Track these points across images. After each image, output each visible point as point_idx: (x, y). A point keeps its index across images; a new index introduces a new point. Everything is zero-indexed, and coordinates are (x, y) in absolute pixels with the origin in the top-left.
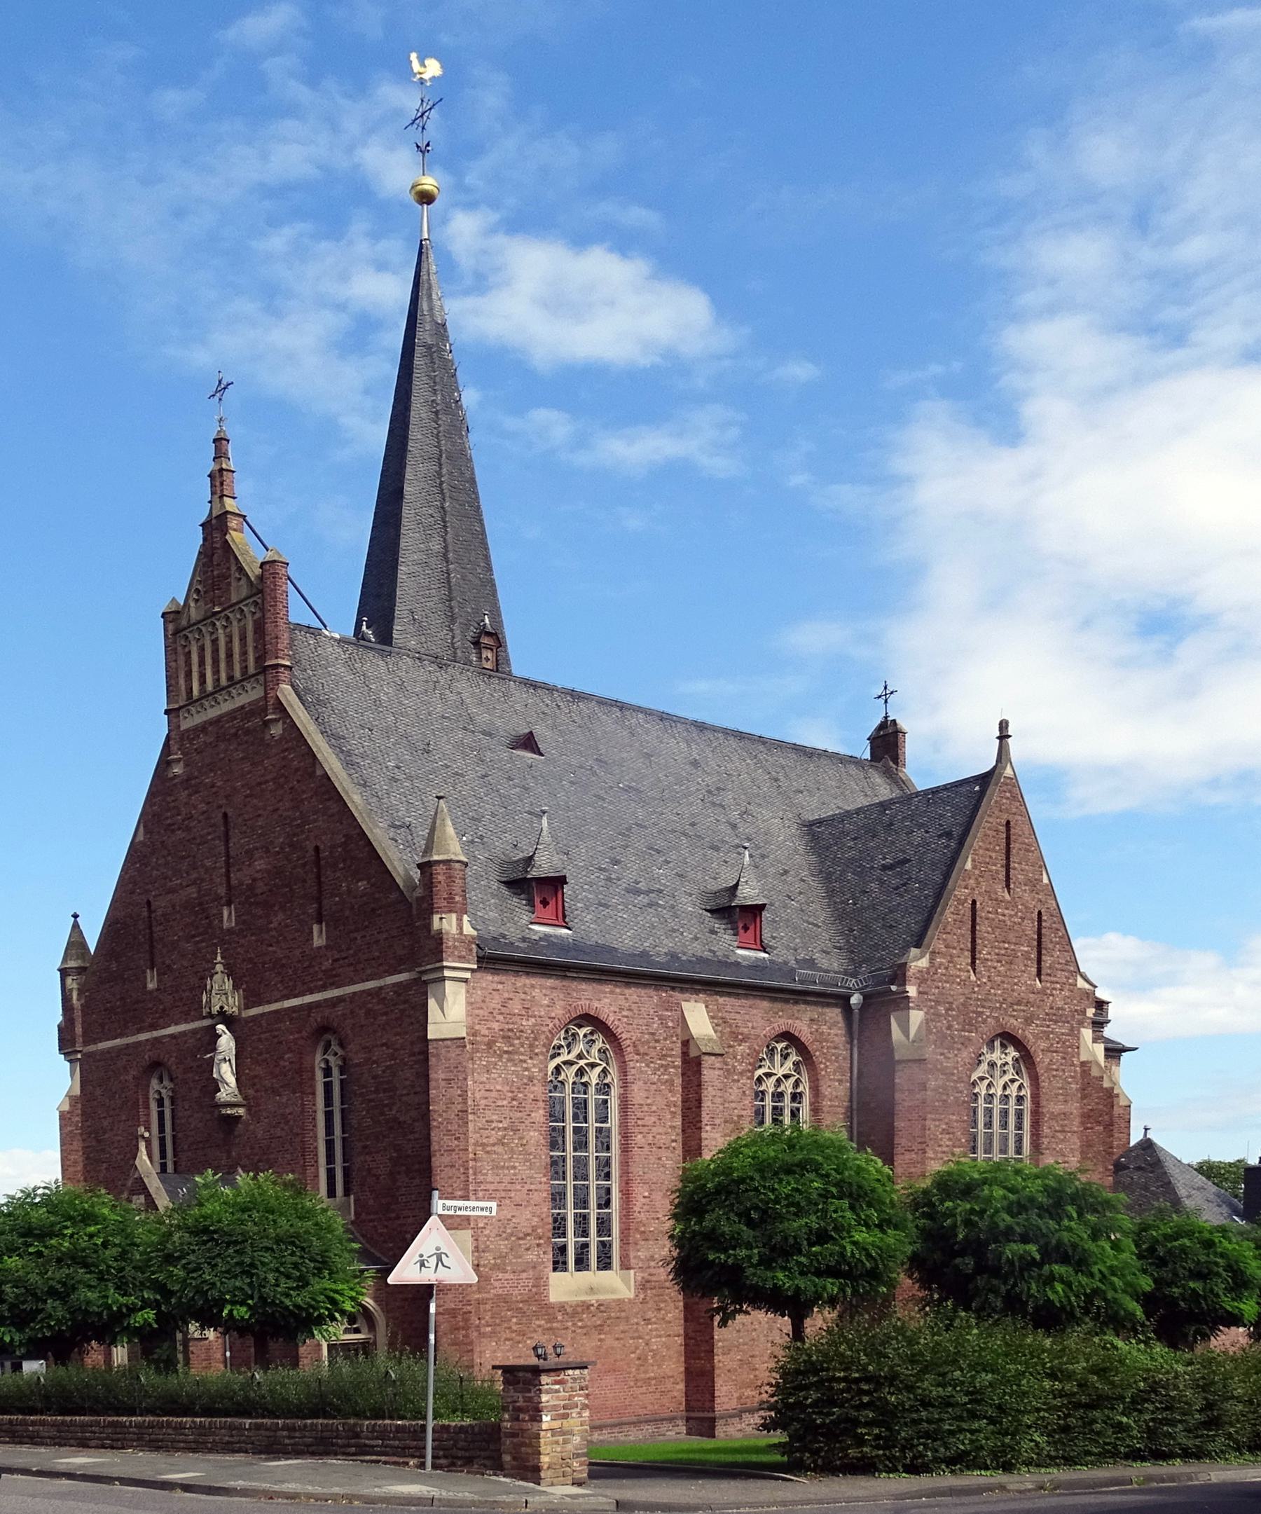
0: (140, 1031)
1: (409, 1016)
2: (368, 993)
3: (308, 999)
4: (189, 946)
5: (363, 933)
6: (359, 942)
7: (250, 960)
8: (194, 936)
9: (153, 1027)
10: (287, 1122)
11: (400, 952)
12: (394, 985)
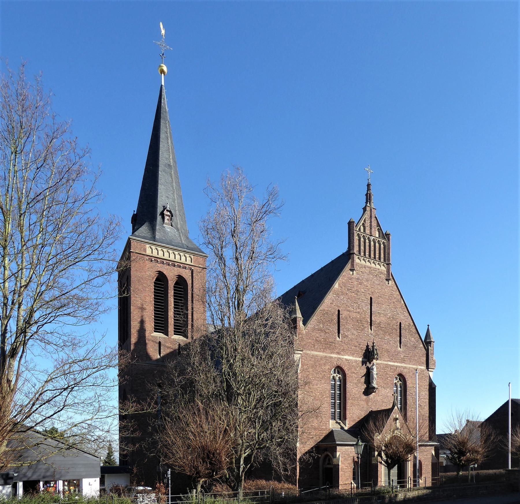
0: (331, 353)
3: (396, 364)
9: (338, 353)
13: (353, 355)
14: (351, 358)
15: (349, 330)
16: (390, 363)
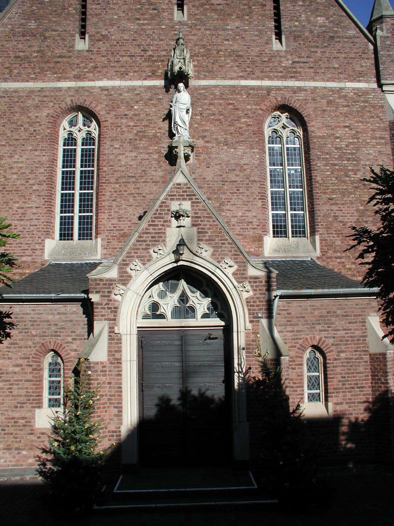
0: (59, 80)
1: (370, 112)
2: (331, 90)
3: (266, 83)
4: (132, 26)
5: (323, 50)
6: (319, 54)
7: (204, 46)
8: (139, 19)
9: (78, 78)
10: (242, 170)
11: (358, 68)
12: (354, 89)
13: (123, 76)
14: (117, 83)
15: (112, 25)
16: (243, 83)
